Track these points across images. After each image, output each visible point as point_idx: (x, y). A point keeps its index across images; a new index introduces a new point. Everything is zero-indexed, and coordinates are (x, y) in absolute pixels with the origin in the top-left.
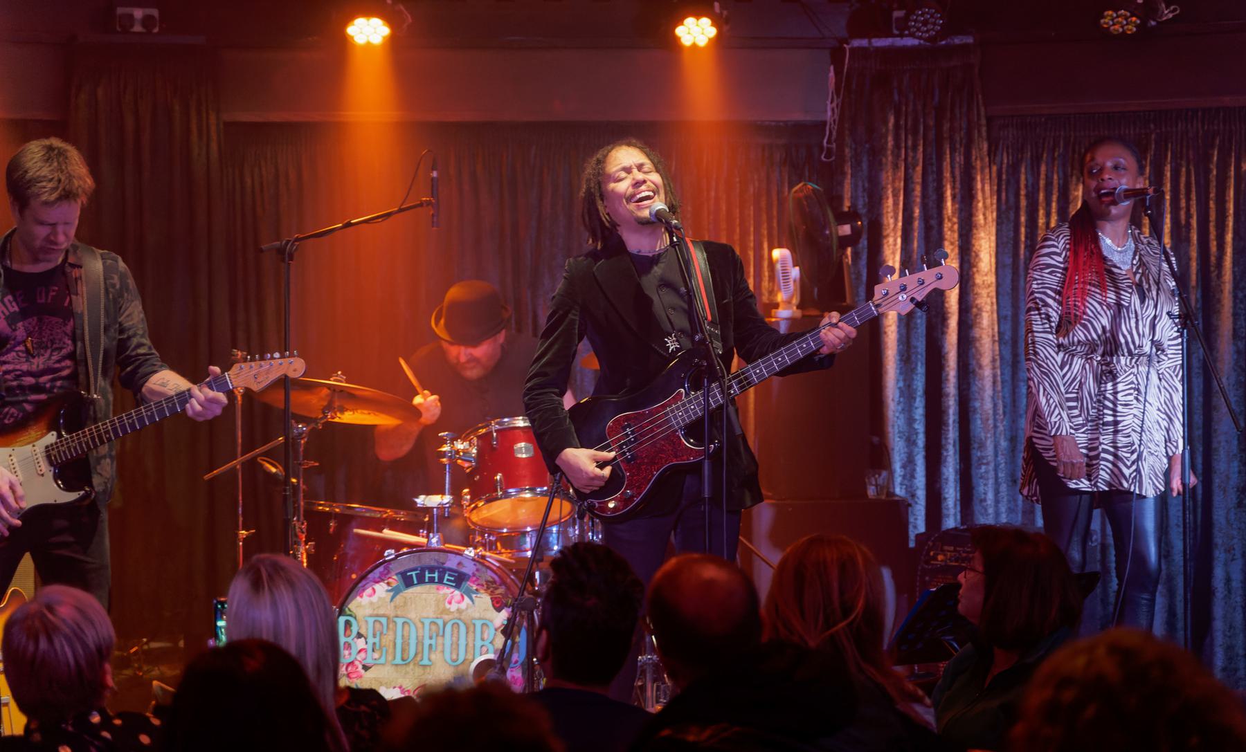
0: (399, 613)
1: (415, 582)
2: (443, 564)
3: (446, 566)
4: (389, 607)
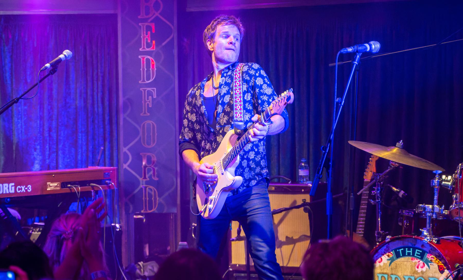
0: (393, 272)
1: (401, 255)
2: (415, 245)
3: (416, 246)
4: (388, 269)
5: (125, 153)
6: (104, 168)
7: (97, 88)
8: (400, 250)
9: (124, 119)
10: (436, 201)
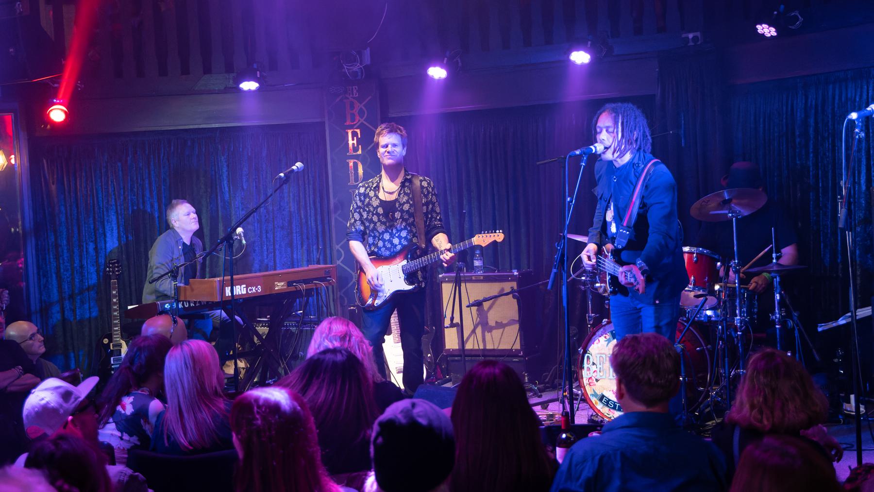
5: (338, 251)
6: (319, 266)
9: (336, 219)
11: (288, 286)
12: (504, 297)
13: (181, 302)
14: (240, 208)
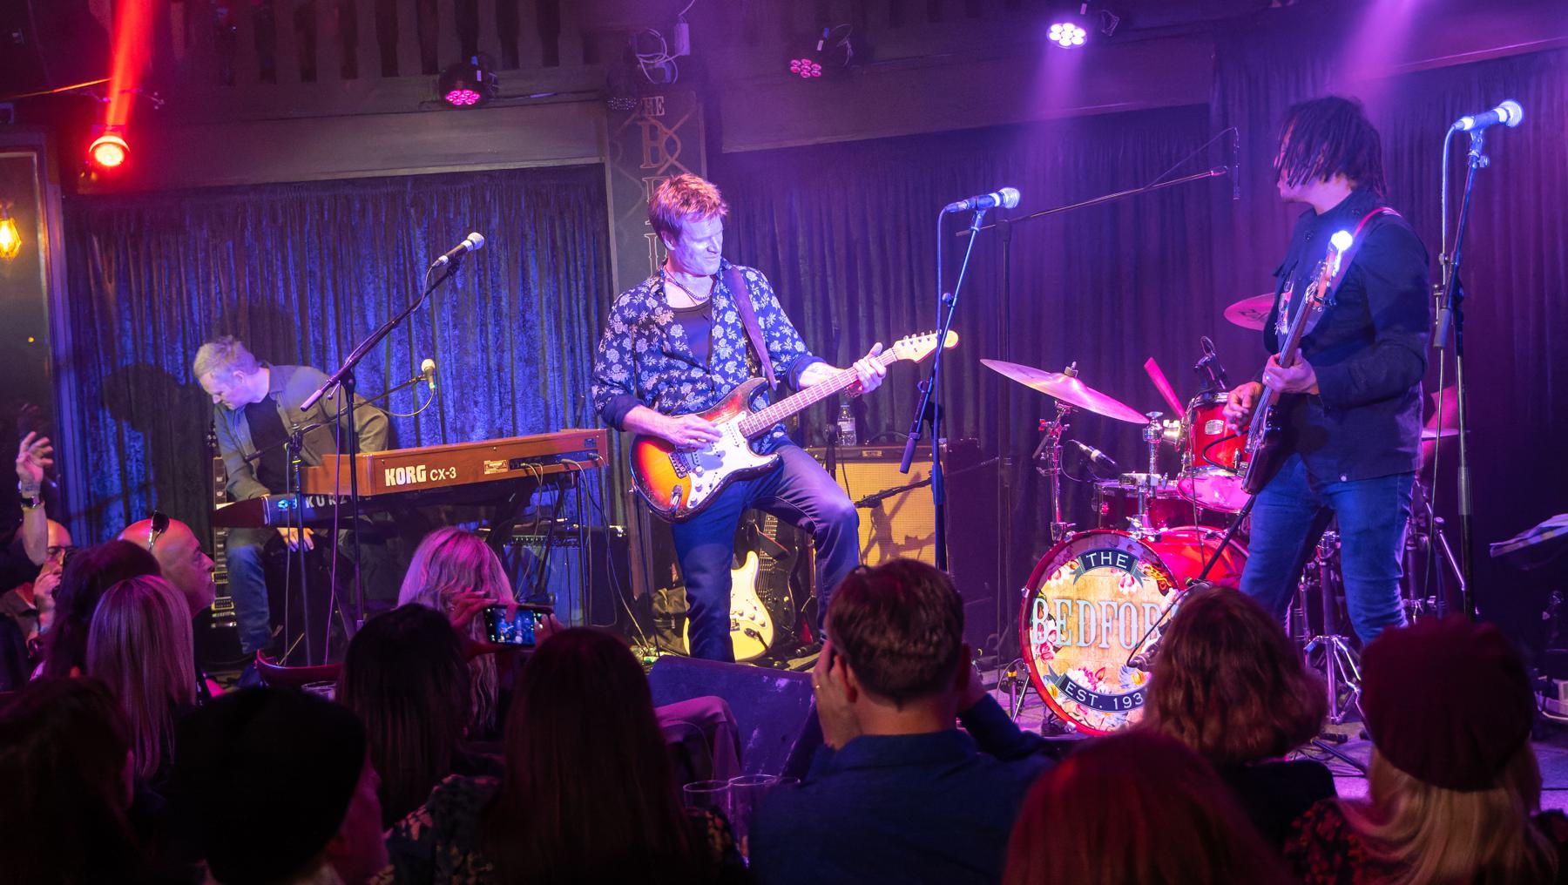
0: (1081, 595)
7: (577, 295)
8: (1091, 556)
10: (1152, 468)
11: (511, 468)
12: (917, 489)
13: (311, 498)
14: (451, 324)
